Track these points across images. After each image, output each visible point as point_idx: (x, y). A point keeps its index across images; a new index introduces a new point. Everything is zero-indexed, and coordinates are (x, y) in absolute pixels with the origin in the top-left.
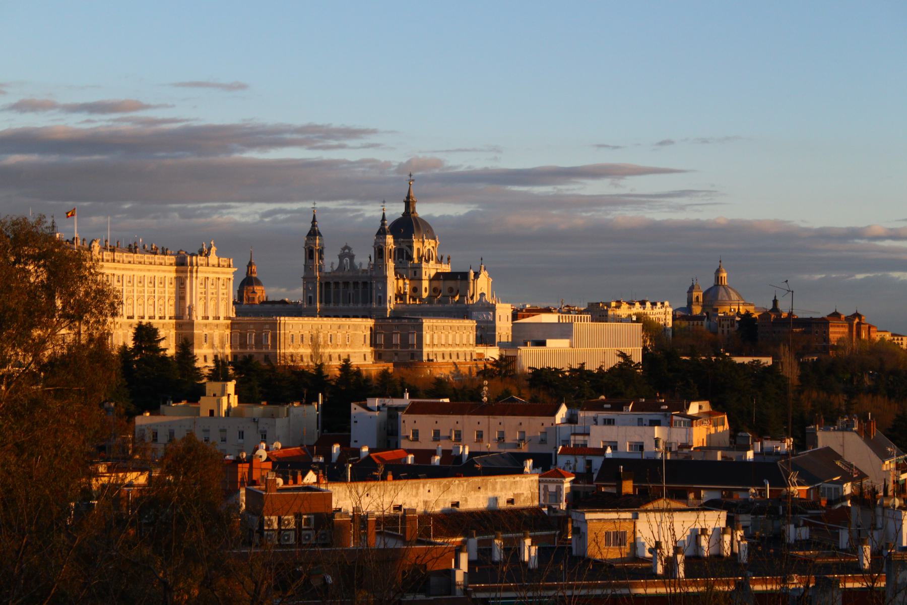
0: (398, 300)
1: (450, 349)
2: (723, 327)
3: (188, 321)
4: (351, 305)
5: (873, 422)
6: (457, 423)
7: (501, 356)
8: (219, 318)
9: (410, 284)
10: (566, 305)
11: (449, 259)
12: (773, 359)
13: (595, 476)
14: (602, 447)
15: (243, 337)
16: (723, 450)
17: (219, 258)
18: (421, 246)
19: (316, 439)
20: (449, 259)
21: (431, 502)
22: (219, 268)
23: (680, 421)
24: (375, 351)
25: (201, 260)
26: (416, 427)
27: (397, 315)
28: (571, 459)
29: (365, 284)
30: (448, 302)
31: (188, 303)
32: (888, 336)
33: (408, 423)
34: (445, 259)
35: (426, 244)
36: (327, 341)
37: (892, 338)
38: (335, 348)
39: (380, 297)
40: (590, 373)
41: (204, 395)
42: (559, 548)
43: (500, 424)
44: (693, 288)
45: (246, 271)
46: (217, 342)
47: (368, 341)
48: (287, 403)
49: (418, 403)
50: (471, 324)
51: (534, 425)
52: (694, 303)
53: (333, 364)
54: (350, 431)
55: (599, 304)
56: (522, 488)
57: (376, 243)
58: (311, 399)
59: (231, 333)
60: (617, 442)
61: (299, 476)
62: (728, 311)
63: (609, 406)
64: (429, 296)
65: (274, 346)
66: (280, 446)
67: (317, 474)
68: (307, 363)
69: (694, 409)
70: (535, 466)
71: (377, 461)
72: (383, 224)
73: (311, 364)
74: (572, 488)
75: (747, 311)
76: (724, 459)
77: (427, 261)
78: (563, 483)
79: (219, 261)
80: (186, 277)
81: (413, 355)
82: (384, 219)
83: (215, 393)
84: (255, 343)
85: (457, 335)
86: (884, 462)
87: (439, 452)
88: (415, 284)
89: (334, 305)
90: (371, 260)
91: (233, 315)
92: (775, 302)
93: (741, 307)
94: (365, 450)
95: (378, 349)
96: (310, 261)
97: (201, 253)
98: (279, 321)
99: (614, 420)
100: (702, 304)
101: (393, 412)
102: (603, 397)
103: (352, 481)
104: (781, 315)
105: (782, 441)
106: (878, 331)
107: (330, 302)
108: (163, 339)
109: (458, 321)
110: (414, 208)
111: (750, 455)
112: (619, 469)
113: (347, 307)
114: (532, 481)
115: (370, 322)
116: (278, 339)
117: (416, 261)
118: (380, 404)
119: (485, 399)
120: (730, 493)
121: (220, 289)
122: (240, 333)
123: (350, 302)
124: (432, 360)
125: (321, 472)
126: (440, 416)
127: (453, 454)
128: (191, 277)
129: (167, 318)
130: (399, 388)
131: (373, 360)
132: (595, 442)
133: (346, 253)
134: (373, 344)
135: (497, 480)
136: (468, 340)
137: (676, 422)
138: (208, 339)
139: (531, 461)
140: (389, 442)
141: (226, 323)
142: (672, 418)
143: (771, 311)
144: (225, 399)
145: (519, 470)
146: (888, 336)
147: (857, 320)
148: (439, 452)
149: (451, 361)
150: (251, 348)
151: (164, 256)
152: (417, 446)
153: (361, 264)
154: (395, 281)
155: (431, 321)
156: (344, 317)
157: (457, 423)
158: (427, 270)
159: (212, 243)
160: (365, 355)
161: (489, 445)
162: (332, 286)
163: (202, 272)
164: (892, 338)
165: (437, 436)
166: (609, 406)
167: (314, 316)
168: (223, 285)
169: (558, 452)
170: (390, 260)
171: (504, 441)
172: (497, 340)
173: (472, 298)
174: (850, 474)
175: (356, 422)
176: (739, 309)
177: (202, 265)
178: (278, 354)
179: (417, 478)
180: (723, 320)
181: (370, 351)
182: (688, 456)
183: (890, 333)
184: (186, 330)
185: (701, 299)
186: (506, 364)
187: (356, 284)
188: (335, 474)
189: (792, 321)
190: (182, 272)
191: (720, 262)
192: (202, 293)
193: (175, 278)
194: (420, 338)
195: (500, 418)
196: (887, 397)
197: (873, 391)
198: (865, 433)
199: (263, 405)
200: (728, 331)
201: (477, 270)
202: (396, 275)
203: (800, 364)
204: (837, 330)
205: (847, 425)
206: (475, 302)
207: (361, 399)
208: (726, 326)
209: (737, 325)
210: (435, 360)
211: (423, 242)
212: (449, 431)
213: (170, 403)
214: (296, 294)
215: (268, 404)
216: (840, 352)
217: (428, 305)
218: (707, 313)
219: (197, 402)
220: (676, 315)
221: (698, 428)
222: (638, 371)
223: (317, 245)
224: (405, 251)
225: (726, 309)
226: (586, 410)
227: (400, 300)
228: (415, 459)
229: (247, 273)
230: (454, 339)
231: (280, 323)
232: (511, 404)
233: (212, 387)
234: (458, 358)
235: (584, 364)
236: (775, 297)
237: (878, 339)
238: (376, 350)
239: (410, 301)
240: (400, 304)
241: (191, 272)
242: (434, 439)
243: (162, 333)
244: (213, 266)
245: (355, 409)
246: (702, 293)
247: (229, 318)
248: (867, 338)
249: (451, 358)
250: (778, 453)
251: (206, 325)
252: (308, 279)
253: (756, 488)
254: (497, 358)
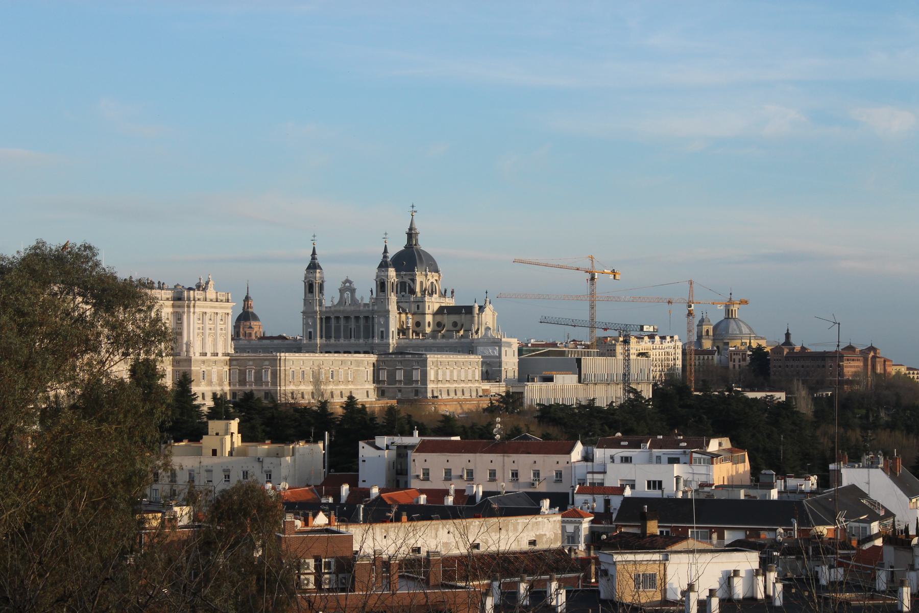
0: (401, 335)
1: (455, 385)
2: (734, 361)
3: (185, 358)
4: (353, 341)
5: (899, 459)
6: (469, 461)
7: (507, 393)
8: (217, 355)
9: (413, 319)
11: (452, 292)
12: (786, 394)
13: (614, 516)
14: (619, 486)
15: (242, 373)
16: (746, 488)
17: (217, 293)
18: (422, 279)
19: (322, 480)
20: (452, 292)
21: (450, 543)
22: (205, 302)
23: (700, 459)
24: (378, 388)
25: (198, 294)
26: (426, 466)
27: (400, 351)
28: (589, 497)
29: (366, 318)
30: (452, 337)
31: (185, 340)
32: (903, 369)
33: (418, 462)
34: (449, 293)
35: (429, 277)
36: (329, 377)
37: (907, 372)
38: (337, 385)
40: (599, 409)
41: (207, 434)
42: (583, 591)
43: (514, 462)
44: (703, 321)
45: (243, 306)
46: (215, 379)
47: (371, 378)
48: (293, 442)
49: (429, 441)
50: (476, 359)
51: (548, 464)
52: (704, 337)
53: (334, 401)
54: (357, 471)
55: (607, 338)
56: (545, 529)
57: (377, 277)
58: (319, 438)
59: (230, 370)
60: (634, 480)
61: (310, 518)
62: (739, 345)
63: (626, 443)
64: (433, 331)
65: (274, 383)
66: (287, 487)
67: (329, 516)
68: (308, 400)
69: (714, 446)
70: (552, 506)
71: (389, 502)
72: (385, 257)
73: (313, 401)
74: (590, 528)
75: (758, 344)
76: (747, 498)
77: (431, 295)
78: (581, 523)
79: (217, 295)
80: (184, 312)
81: (417, 392)
82: (386, 251)
83: (217, 431)
84: (255, 380)
85: (462, 370)
86: (911, 500)
87: (452, 492)
88: (418, 318)
89: (335, 341)
90: (372, 294)
91: (231, 351)
92: (788, 335)
93: (752, 341)
94: (375, 491)
95: (381, 385)
96: (310, 295)
97: (199, 287)
98: (279, 357)
99: (631, 458)
100: (712, 338)
101: (402, 451)
102: (619, 434)
103: (365, 522)
104: (794, 348)
105: (807, 479)
106: (893, 365)
107: (331, 337)
109: (463, 357)
110: (417, 240)
111: (774, 494)
112: (643, 508)
113: (349, 342)
114: (554, 521)
115: (373, 358)
116: (278, 376)
117: (419, 295)
118: (389, 443)
119: (498, 436)
120: (756, 533)
121: (218, 324)
122: (239, 370)
123: (351, 338)
124: (437, 397)
125: (333, 512)
126: (452, 454)
127: (466, 494)
128: (189, 312)
130: (407, 427)
131: (375, 397)
132: (612, 480)
133: (347, 287)
134: (376, 380)
135: (518, 521)
136: (474, 374)
137: (695, 460)
138: (205, 376)
139: (548, 501)
140: (398, 482)
141: (225, 360)
142: (691, 456)
143: (783, 344)
144: (228, 438)
145: (535, 511)
146: (903, 370)
147: (872, 354)
148: (452, 492)
149: (456, 397)
150: (251, 385)
151: (160, 291)
152: (427, 486)
153: (362, 299)
154: (398, 316)
155: (436, 356)
156: (345, 352)
157: (469, 461)
158: (430, 304)
159: (210, 277)
160: (367, 392)
161: (504, 485)
162: (333, 322)
163: (199, 307)
164: (907, 372)
165: (448, 476)
166: (626, 443)
167: (314, 352)
168: (222, 320)
169: (575, 492)
170: (392, 294)
171: (517, 480)
172: (503, 377)
173: (477, 332)
174: (874, 511)
175: (364, 461)
176: (750, 343)
177: (199, 300)
178: (278, 391)
179: (431, 519)
180: (734, 354)
181: (373, 387)
182: (710, 495)
183: (905, 367)
184: (183, 367)
185: (711, 333)
186: (512, 401)
187: (357, 318)
188: (347, 514)
189: (804, 355)
190: (179, 307)
191: (731, 294)
192: (199, 329)
193: (172, 313)
194: (424, 375)
195: (514, 457)
196: (905, 432)
197: (891, 426)
198: (891, 471)
199: (267, 444)
200: (739, 365)
201: (482, 304)
202: (398, 309)
203: (814, 399)
204: (852, 363)
205: (872, 462)
206: (480, 337)
207: (369, 438)
208: (737, 361)
209: (748, 358)
210: (440, 397)
211: (426, 275)
212: (461, 470)
213: (170, 442)
214: (294, 329)
215: (272, 443)
216: (856, 387)
217: (432, 340)
218: (718, 347)
219: (199, 441)
220: (685, 350)
221: (719, 465)
222: (650, 407)
223: (317, 279)
224: (407, 284)
225: (738, 343)
226: (606, 448)
227: (402, 336)
228: (428, 500)
229: (244, 308)
230: (459, 375)
231: (280, 359)
232: (524, 441)
233: (214, 426)
234: (463, 394)
235: (594, 399)
236: (788, 330)
237: (893, 373)
238: (379, 386)
239: (413, 336)
240: (402, 338)
241: (189, 307)
242: (445, 478)
244: (211, 300)
245: (363, 447)
246: (712, 327)
247: (228, 355)
248: (882, 372)
249: (456, 395)
250: (802, 492)
251: (204, 362)
252: (308, 313)
253: (783, 528)
254: (504, 394)
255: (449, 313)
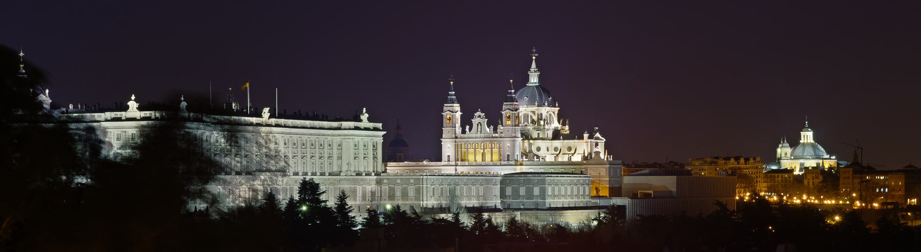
0: (524, 157)
3: (345, 177)
10: (670, 161)
38: (470, 199)
39: (508, 155)
46: (368, 195)
88: (539, 143)
108: (324, 192)
129: (327, 174)
134: (503, 195)
178: (421, 205)
200: (813, 182)
202: (522, 135)
231: (422, 179)
243: (322, 188)
255: (564, 139)
